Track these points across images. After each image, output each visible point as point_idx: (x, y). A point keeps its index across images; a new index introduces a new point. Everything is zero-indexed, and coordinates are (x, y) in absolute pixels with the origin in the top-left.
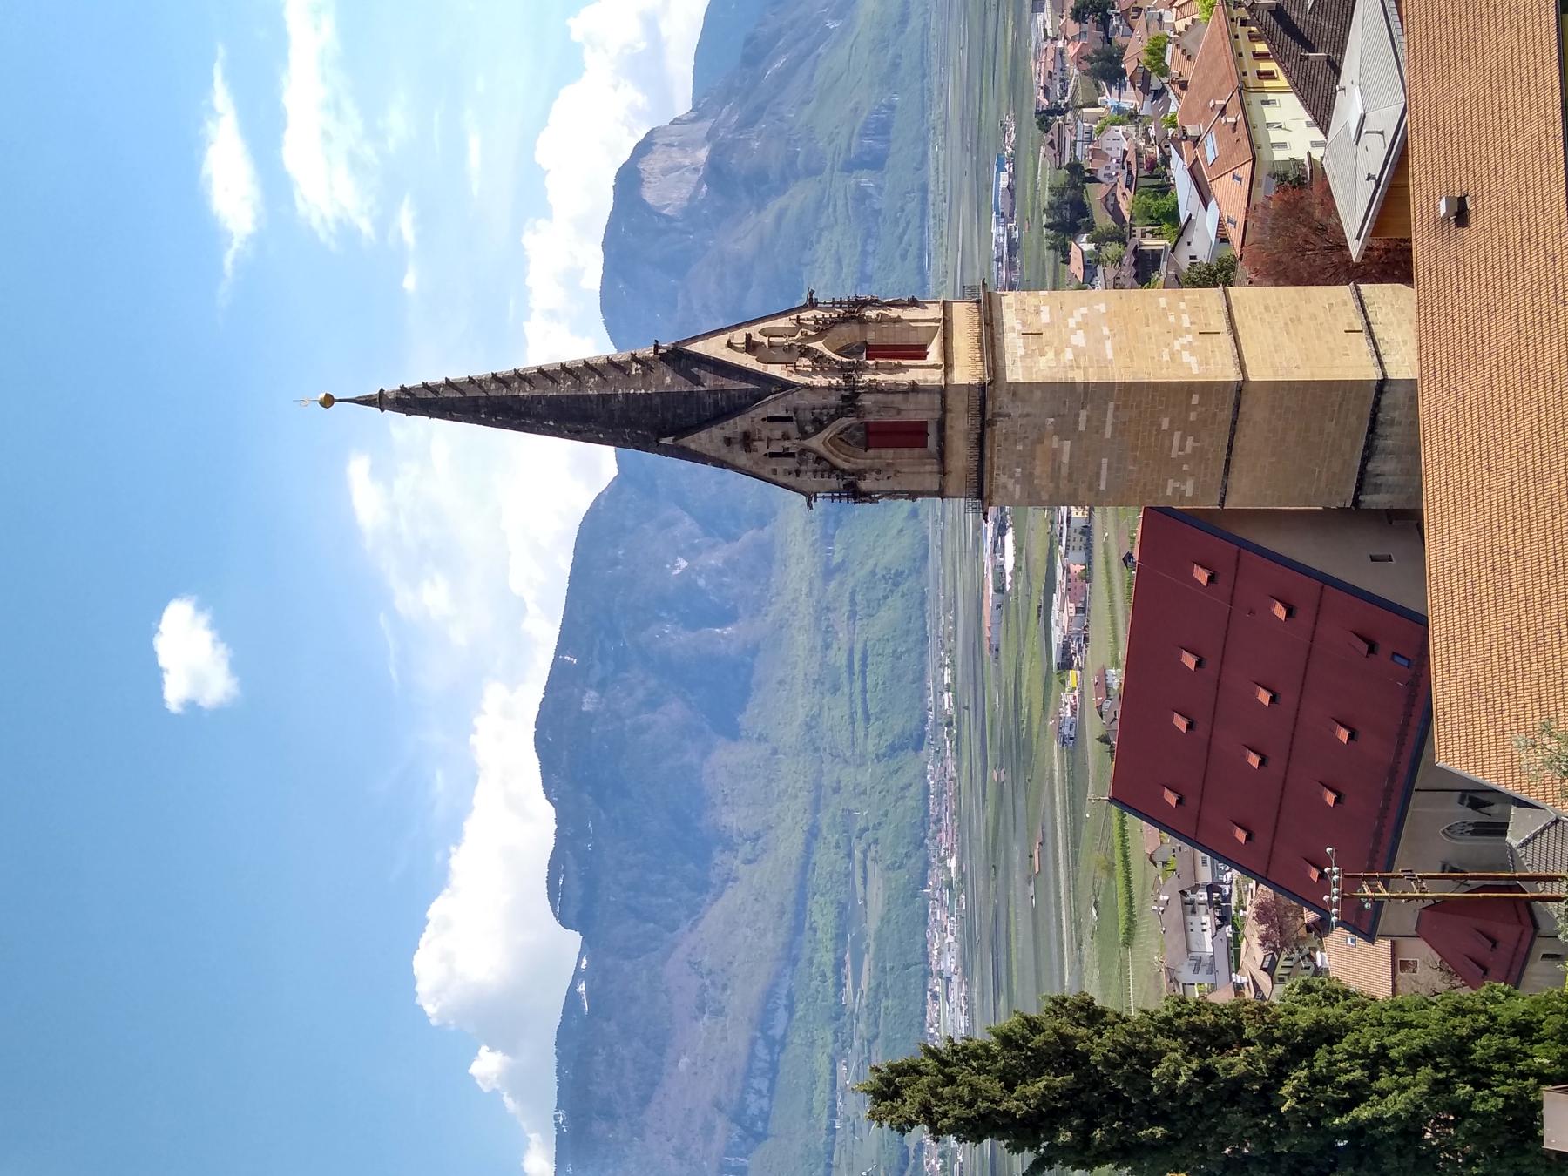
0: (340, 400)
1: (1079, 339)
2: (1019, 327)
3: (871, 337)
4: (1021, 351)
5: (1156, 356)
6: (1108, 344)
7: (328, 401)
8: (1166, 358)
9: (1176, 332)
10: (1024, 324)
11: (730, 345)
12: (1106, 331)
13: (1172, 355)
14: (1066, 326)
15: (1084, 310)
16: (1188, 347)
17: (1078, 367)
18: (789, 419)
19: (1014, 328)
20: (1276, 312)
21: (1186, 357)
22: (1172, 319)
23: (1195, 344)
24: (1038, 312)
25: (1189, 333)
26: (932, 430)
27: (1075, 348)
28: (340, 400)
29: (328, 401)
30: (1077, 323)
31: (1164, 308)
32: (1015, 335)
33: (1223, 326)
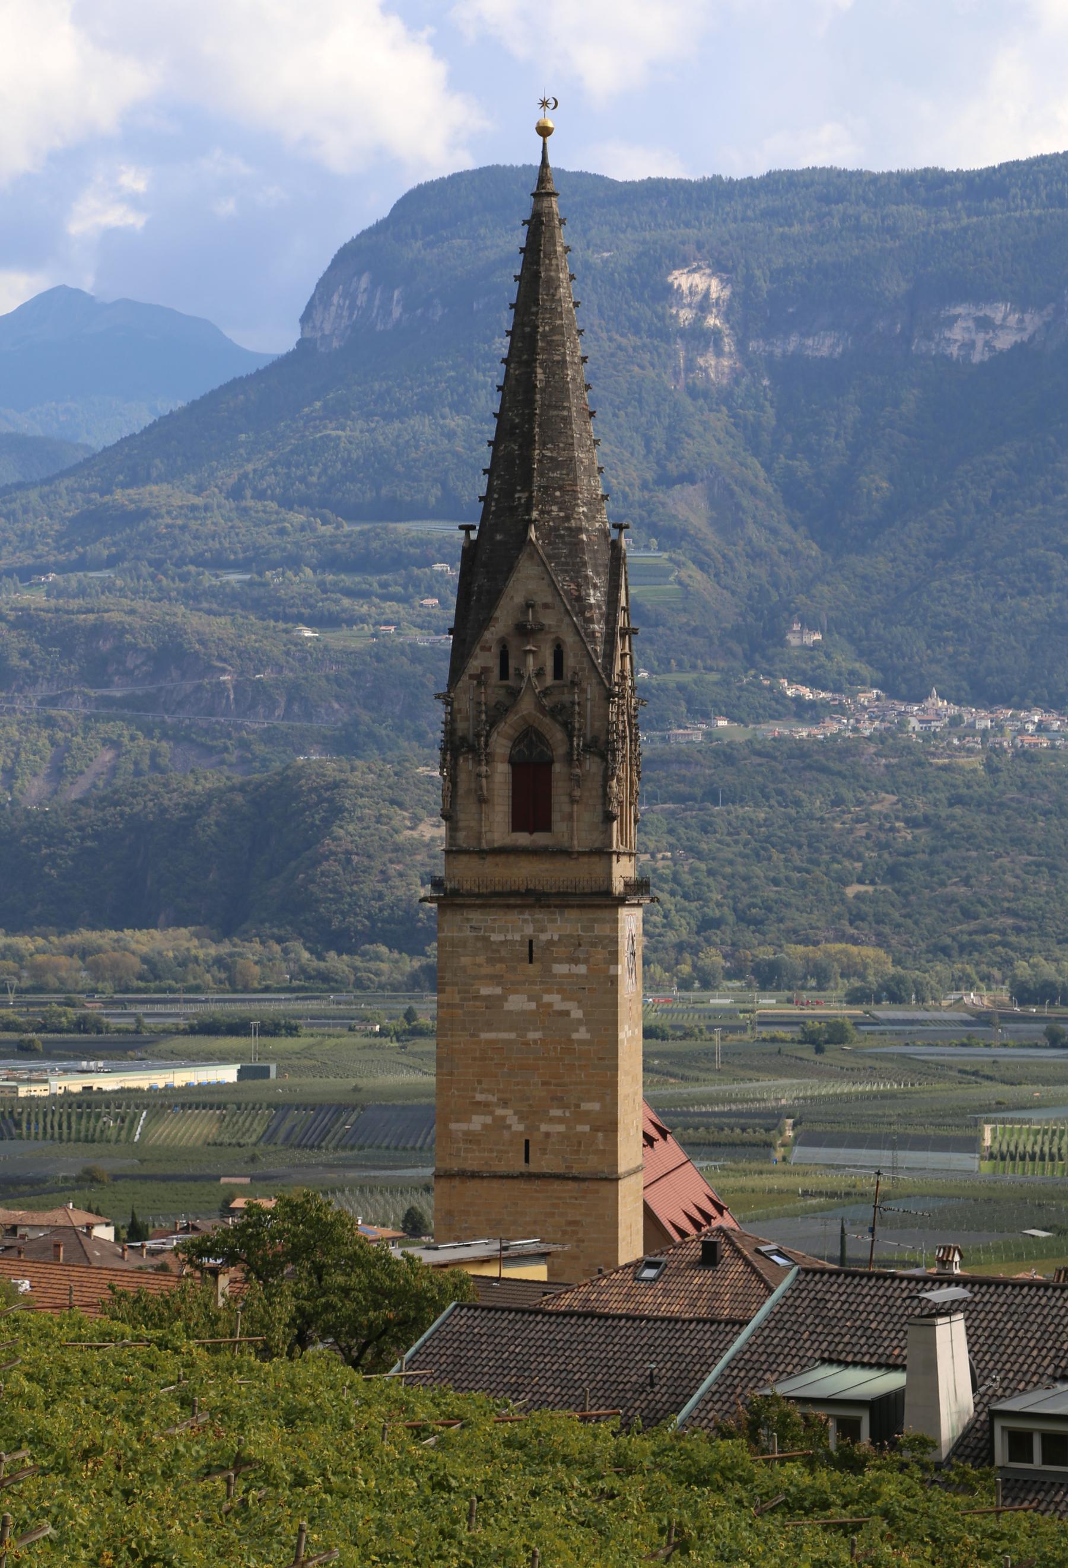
0: (544, 144)
1: (517, 1002)
2: (544, 937)
3: (557, 768)
4: (495, 937)
5: (484, 1086)
6: (513, 1036)
7: (544, 131)
8: (479, 1097)
9: (531, 1115)
10: (551, 943)
11: (529, 605)
12: (532, 1035)
13: (487, 1105)
14: (548, 991)
15: (577, 1014)
16: (500, 1124)
17: (463, 999)
18: (558, 673)
19: (543, 930)
20: (564, 1233)
21: (477, 1122)
22: (556, 1112)
23: (506, 1134)
24: (576, 961)
25: (527, 1127)
26: (541, 839)
27: (503, 998)
28: (544, 144)
29: (544, 131)
30: (550, 1005)
31: (578, 1106)
32: (529, 930)
33: (533, 1168)
